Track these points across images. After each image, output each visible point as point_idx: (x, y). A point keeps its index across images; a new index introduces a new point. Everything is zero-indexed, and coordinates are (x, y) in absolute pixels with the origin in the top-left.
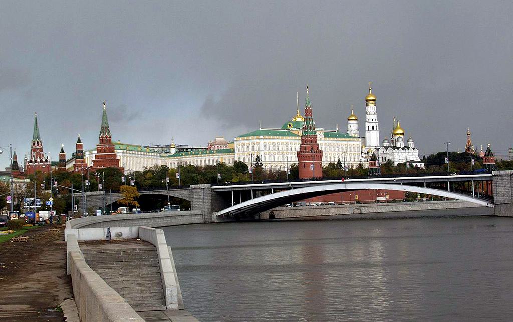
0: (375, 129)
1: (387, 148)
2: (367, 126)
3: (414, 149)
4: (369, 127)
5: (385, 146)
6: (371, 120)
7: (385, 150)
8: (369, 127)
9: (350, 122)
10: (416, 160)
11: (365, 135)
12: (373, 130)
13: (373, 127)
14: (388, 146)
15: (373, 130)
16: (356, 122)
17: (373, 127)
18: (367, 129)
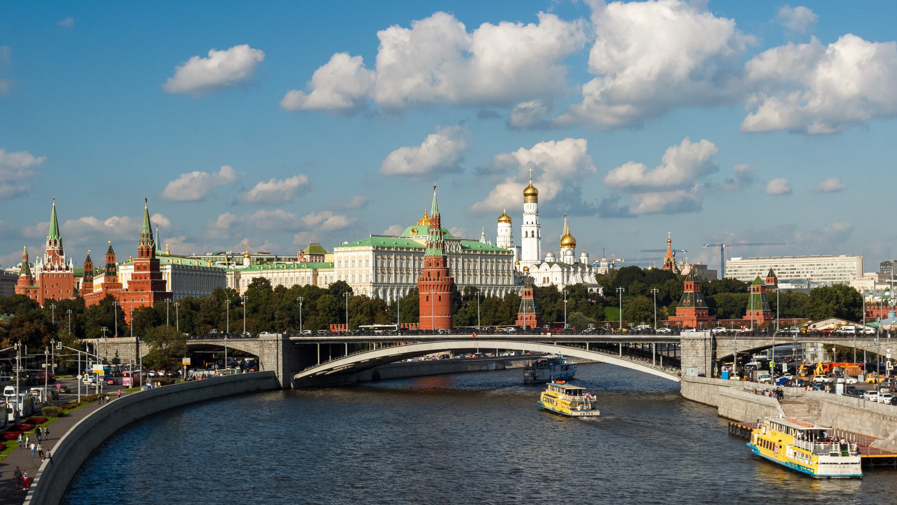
0: (536, 235)
2: (524, 230)
5: (549, 261)
6: (530, 223)
7: (548, 267)
8: (527, 233)
12: (533, 236)
13: (533, 232)
14: (552, 261)
15: (533, 236)
17: (533, 232)
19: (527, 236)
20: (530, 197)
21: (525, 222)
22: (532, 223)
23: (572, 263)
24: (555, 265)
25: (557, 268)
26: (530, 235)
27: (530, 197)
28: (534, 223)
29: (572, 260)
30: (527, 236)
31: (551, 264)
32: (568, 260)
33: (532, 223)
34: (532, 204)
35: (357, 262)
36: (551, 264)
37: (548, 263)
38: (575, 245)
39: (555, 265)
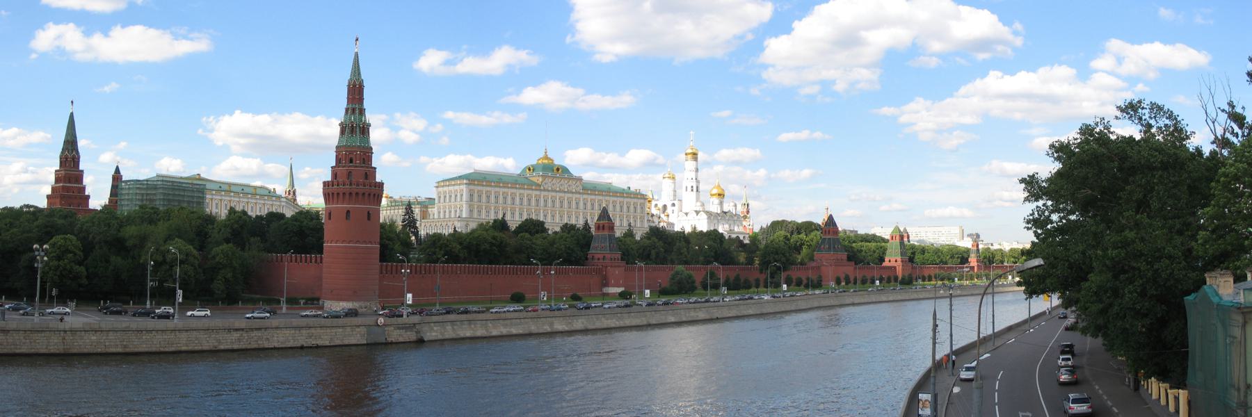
5: (698, 209)
8: (687, 187)
12: (692, 190)
13: (692, 187)
15: (692, 190)
17: (692, 187)
19: (686, 190)
20: (689, 156)
24: (702, 212)
25: (703, 216)
26: (689, 189)
27: (689, 156)
28: (694, 178)
31: (697, 212)
35: (453, 196)
36: (697, 212)
37: (696, 211)
38: (724, 195)
39: (702, 212)
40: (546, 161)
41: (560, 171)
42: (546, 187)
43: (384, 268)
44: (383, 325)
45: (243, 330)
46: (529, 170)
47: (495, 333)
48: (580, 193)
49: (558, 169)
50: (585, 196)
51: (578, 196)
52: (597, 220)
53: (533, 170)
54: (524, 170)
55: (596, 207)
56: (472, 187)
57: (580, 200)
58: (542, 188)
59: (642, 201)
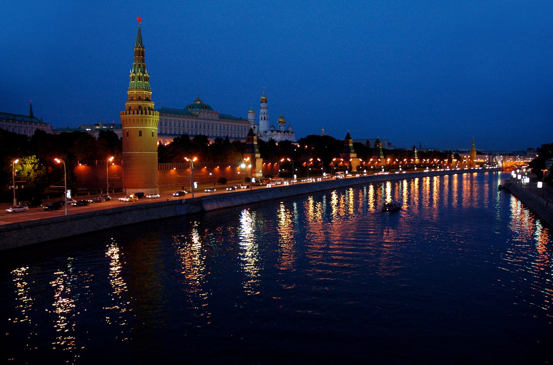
0: (266, 118)
1: (272, 131)
2: (260, 117)
3: (292, 133)
4: (262, 117)
5: (272, 130)
7: (271, 133)
8: (262, 117)
9: (249, 114)
10: (293, 141)
11: (259, 123)
13: (265, 117)
14: (273, 130)
16: (253, 114)
17: (265, 117)
18: (260, 119)
19: (262, 119)
21: (261, 113)
22: (265, 113)
23: (283, 131)
26: (263, 119)
29: (283, 129)
30: (262, 119)
32: (282, 129)
33: (265, 113)
34: (264, 104)
36: (272, 131)
37: (271, 131)
39: (275, 131)
40: (198, 102)
41: (207, 108)
42: (200, 117)
43: (160, 166)
44: (185, 203)
45: (111, 214)
46: (190, 107)
47: (236, 204)
48: (218, 121)
49: (206, 107)
50: (221, 122)
51: (217, 122)
52: (247, 136)
53: (192, 107)
54: (187, 108)
55: (247, 128)
56: (162, 117)
57: (218, 125)
58: (198, 118)
59: (248, 125)
